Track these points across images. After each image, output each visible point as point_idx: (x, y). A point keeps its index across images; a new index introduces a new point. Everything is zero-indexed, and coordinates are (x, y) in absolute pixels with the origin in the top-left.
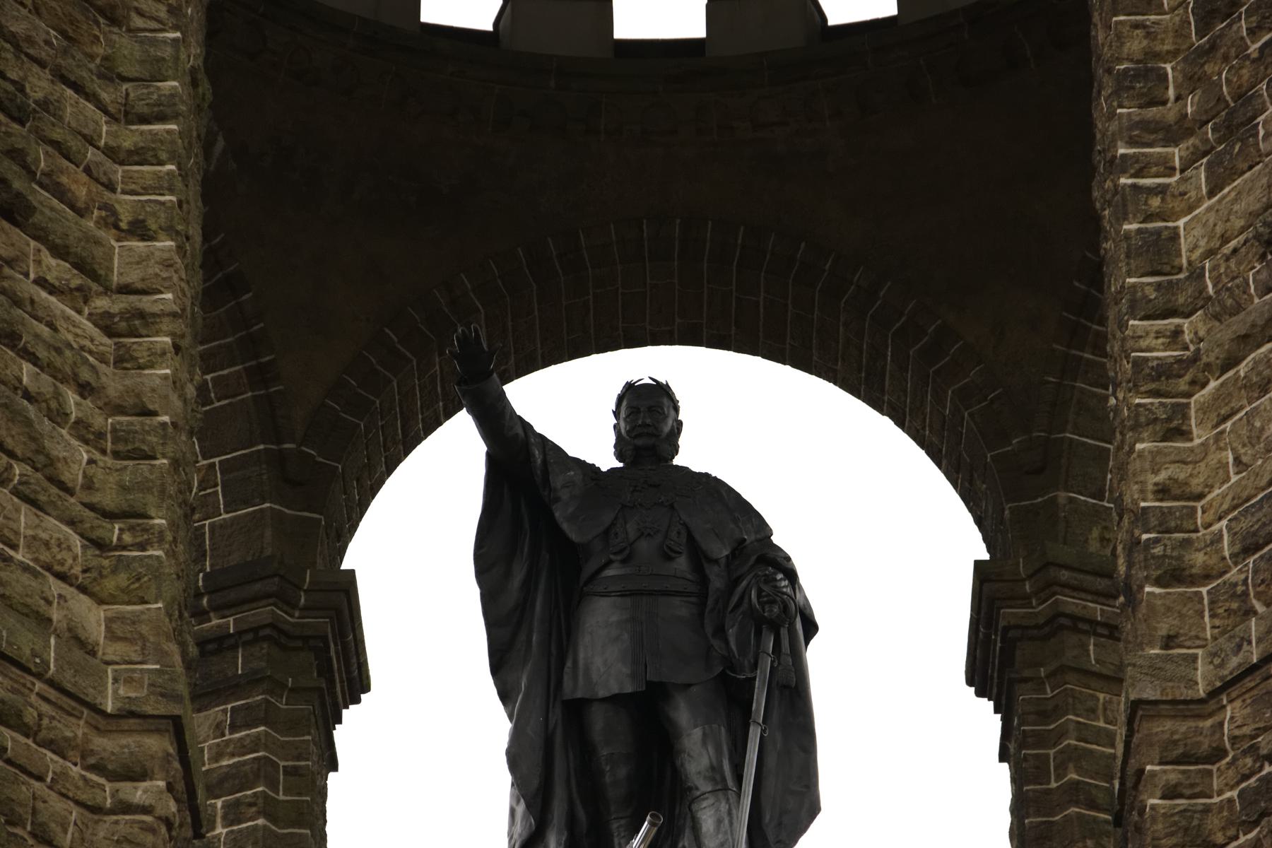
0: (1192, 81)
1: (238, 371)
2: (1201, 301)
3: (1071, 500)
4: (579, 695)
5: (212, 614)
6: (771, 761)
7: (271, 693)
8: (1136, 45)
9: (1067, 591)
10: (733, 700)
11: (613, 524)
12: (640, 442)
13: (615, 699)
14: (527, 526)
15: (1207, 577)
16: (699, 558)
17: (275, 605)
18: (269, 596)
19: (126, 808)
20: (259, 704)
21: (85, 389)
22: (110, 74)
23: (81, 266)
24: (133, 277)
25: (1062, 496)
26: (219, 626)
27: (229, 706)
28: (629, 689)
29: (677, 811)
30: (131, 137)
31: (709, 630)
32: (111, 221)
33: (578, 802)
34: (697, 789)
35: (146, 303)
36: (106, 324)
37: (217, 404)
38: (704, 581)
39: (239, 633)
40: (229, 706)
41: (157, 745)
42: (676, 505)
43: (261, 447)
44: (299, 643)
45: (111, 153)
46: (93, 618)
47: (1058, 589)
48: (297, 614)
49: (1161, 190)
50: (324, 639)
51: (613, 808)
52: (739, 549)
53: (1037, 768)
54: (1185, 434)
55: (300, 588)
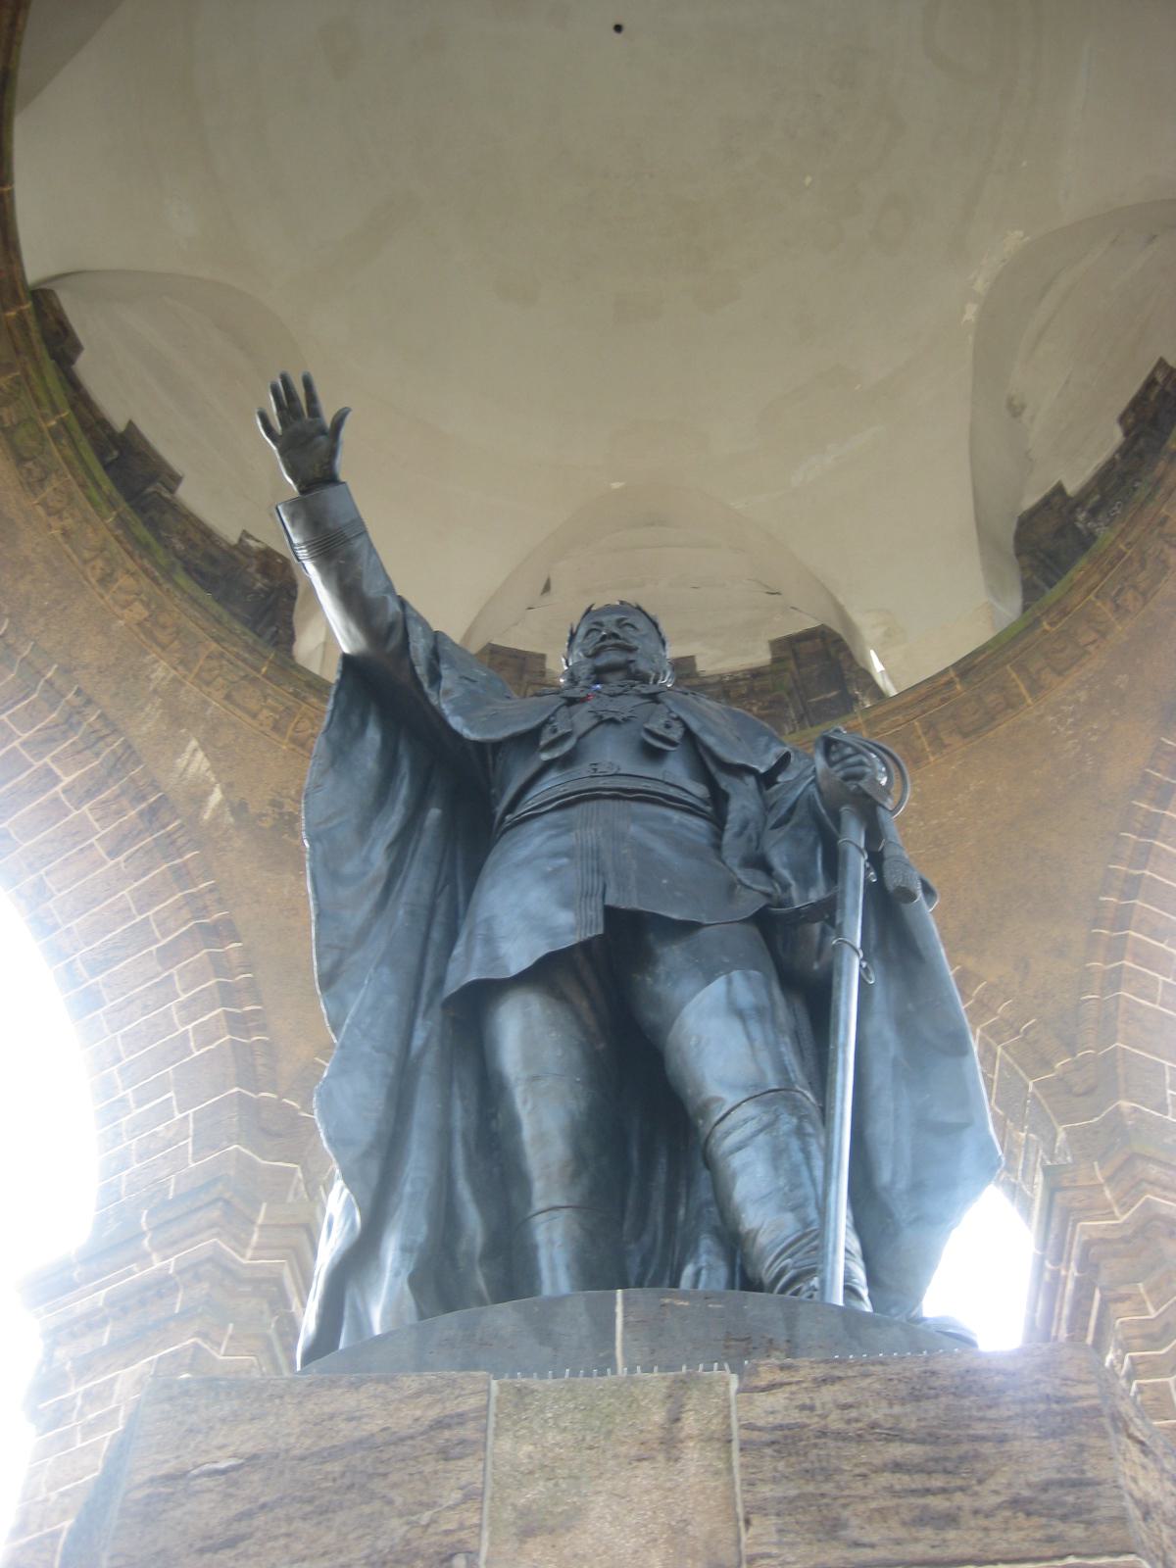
1: (217, 1015)
3: (1136, 1110)
4: (473, 977)
5: (154, 1257)
6: (881, 1074)
7: (205, 1336)
9: (1158, 1190)
11: (546, 722)
12: (602, 661)
13: (544, 974)
14: (405, 767)
16: (704, 762)
17: (218, 1235)
18: (211, 1226)
20: (185, 1349)
25: (1125, 1105)
26: (160, 1269)
27: (156, 1356)
28: (572, 940)
29: (682, 1212)
31: (733, 861)
33: (464, 1190)
34: (718, 1099)
37: (197, 1054)
38: (719, 799)
39: (179, 1272)
40: (156, 1356)
42: (660, 696)
43: (236, 1090)
44: (248, 1289)
47: (1145, 1185)
48: (249, 1253)
50: (278, 1282)
51: (538, 1186)
53: (1157, 1399)
55: (253, 1222)
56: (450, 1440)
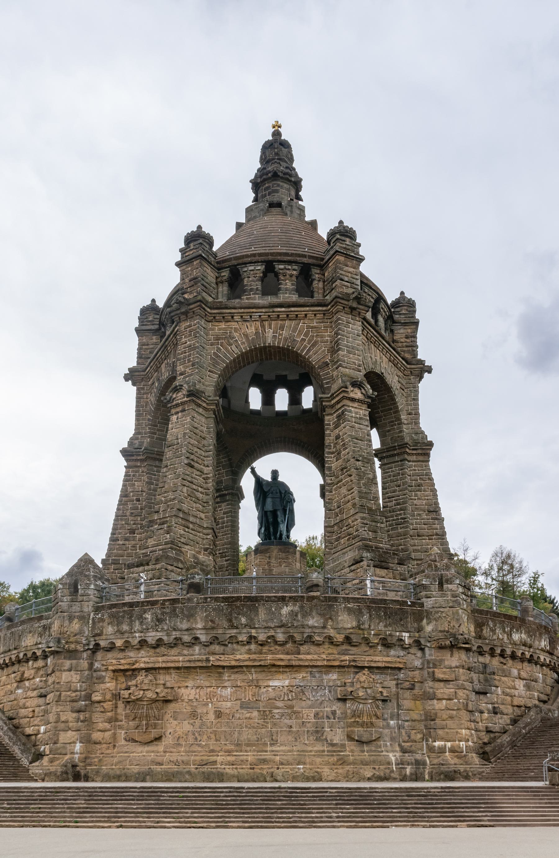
0: (335, 447)
2: (334, 475)
8: (328, 441)
10: (285, 511)
15: (334, 510)
19: (207, 539)
21: (201, 487)
22: (204, 446)
23: (201, 472)
24: (207, 472)
30: (207, 454)
32: (204, 465)
35: (209, 476)
36: (204, 478)
41: (211, 531)
45: (204, 456)
46: (203, 516)
49: (330, 461)
52: (286, 491)
54: (332, 492)
56: (269, 548)
